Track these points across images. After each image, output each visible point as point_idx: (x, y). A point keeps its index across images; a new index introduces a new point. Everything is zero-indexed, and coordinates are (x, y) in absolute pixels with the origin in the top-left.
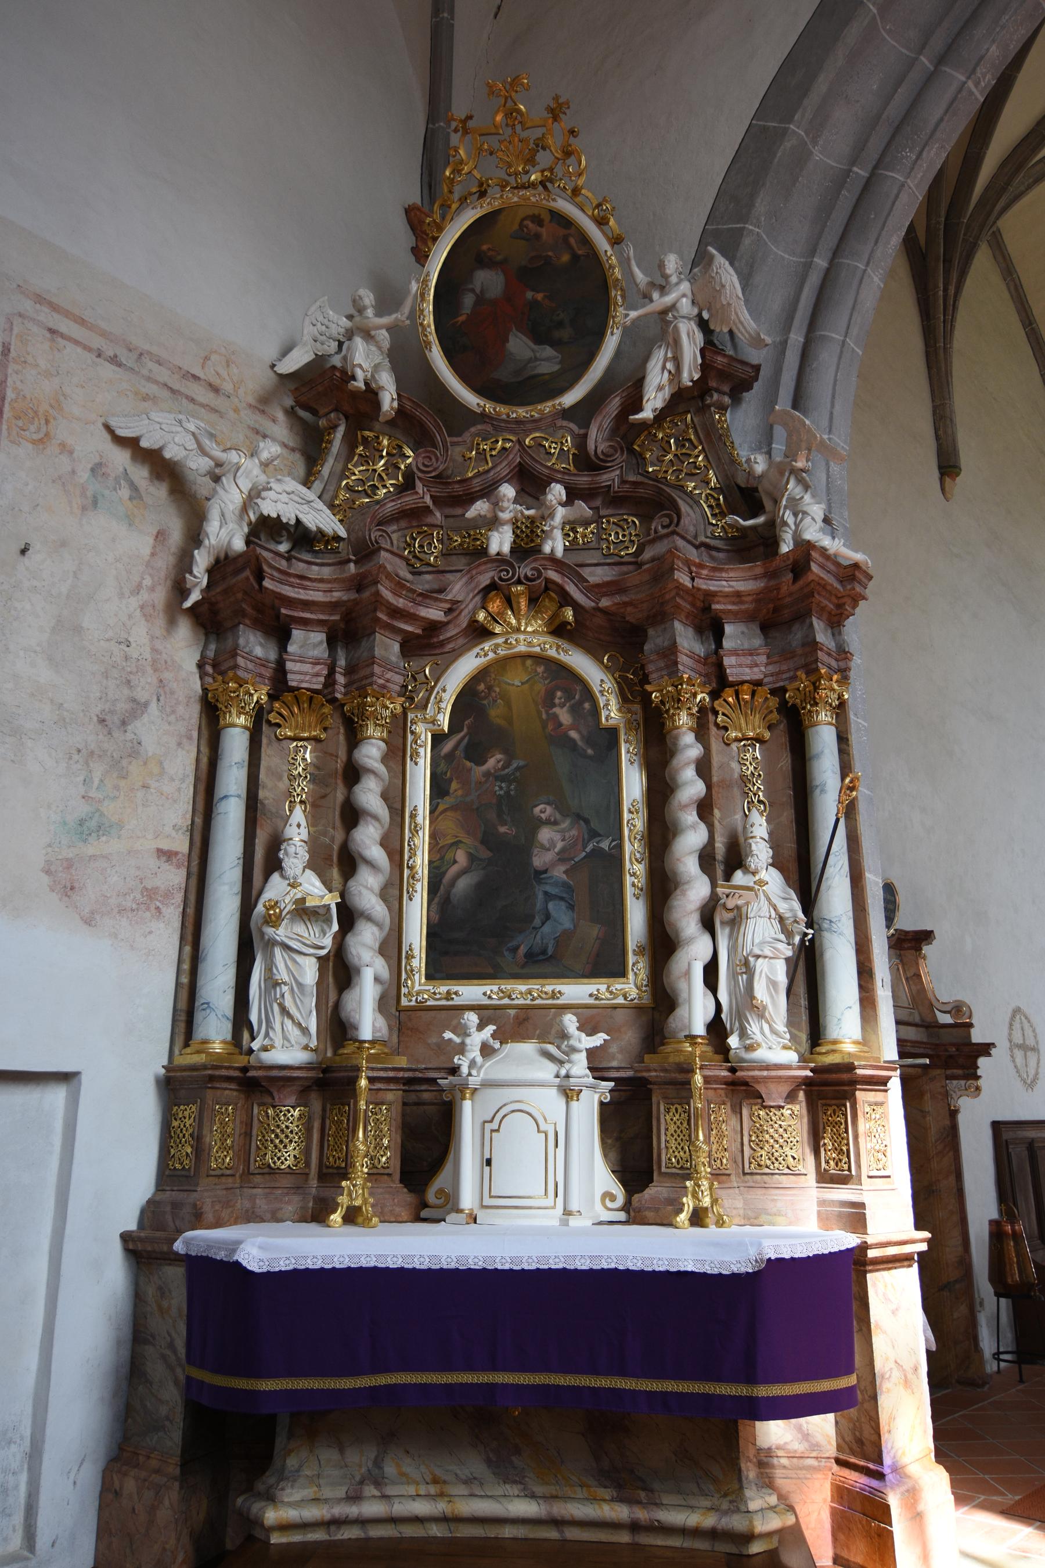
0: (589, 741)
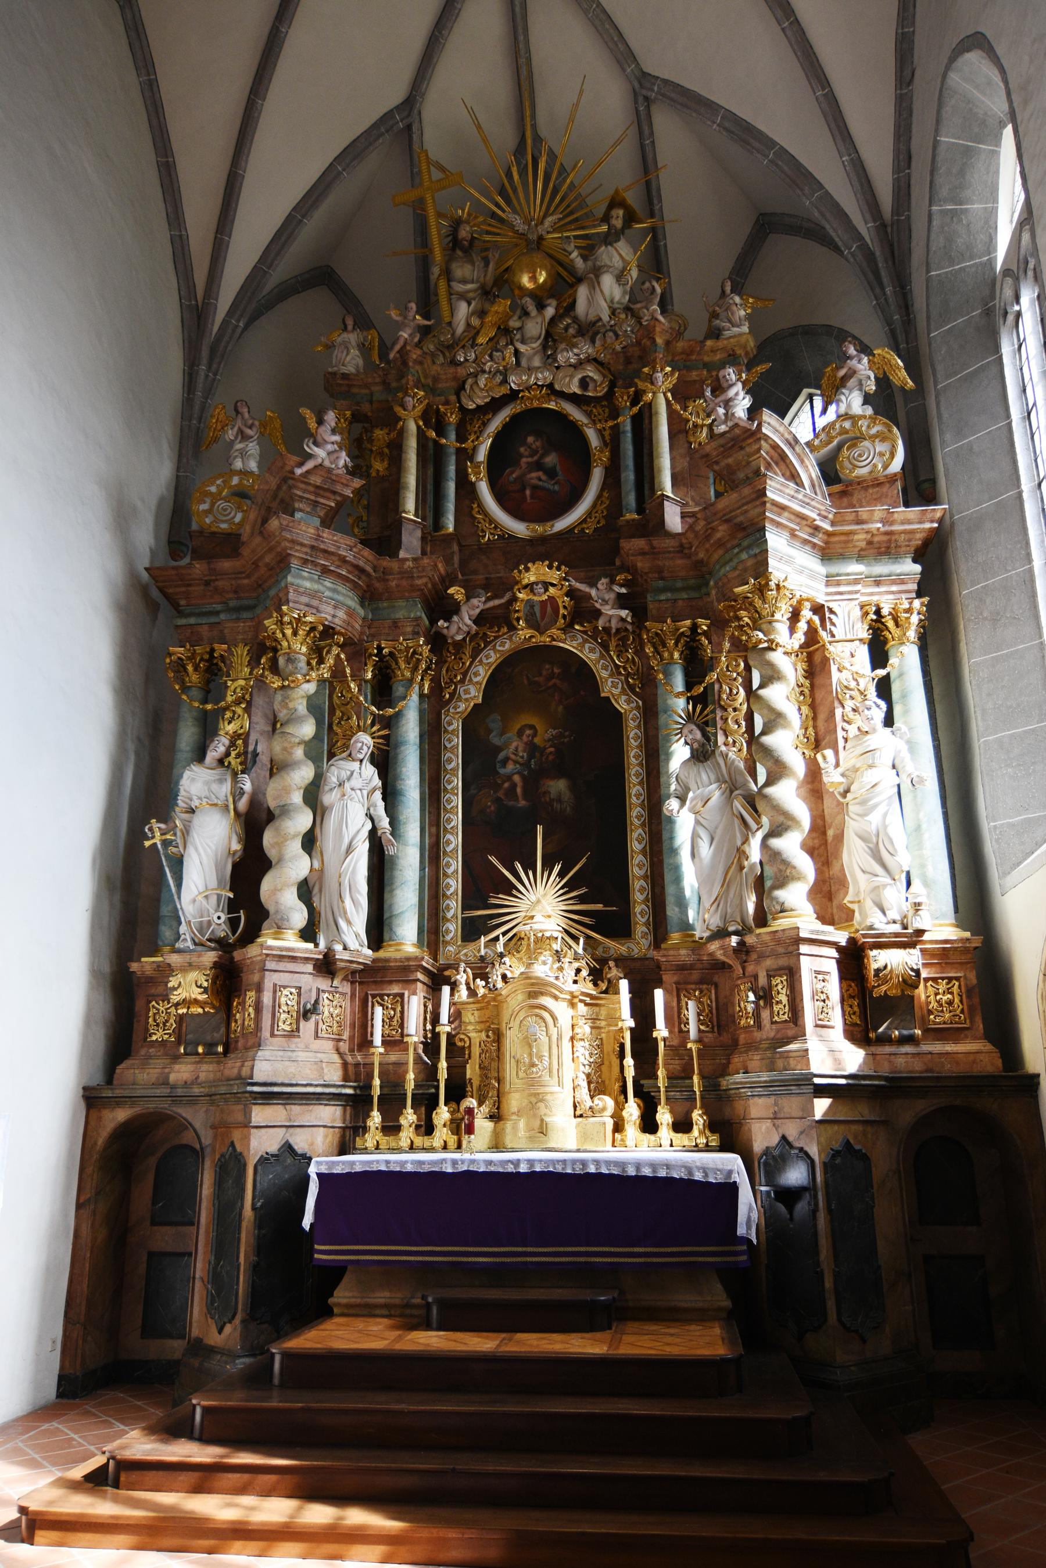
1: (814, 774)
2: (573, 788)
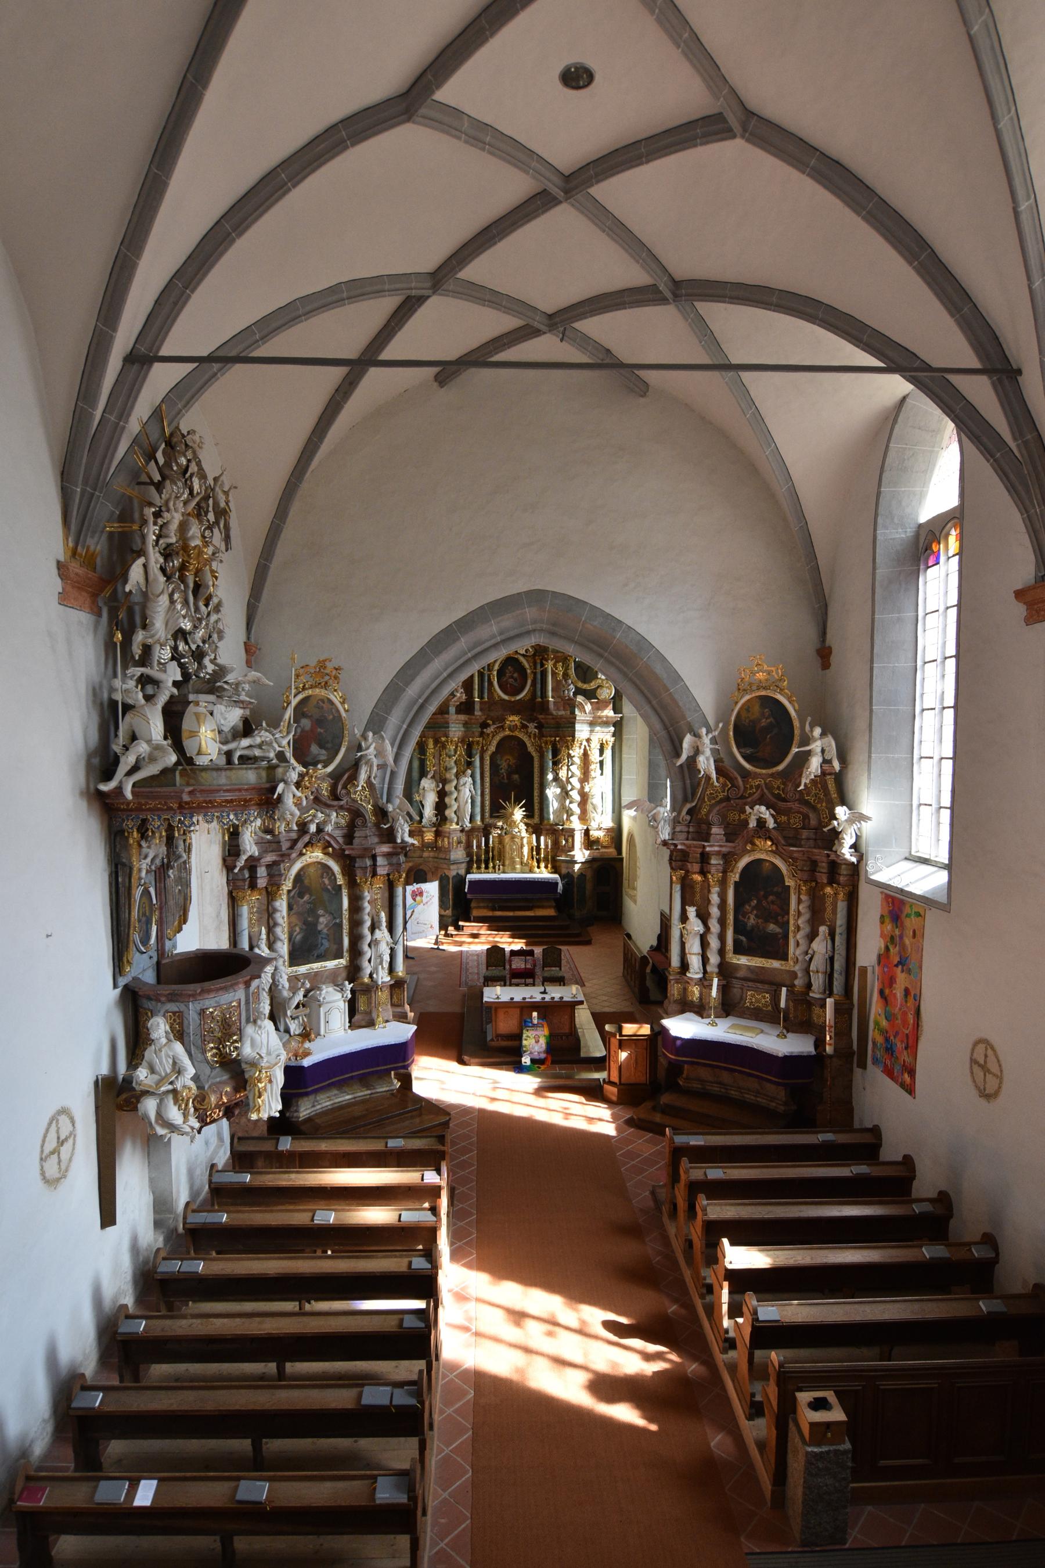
1: (582, 788)
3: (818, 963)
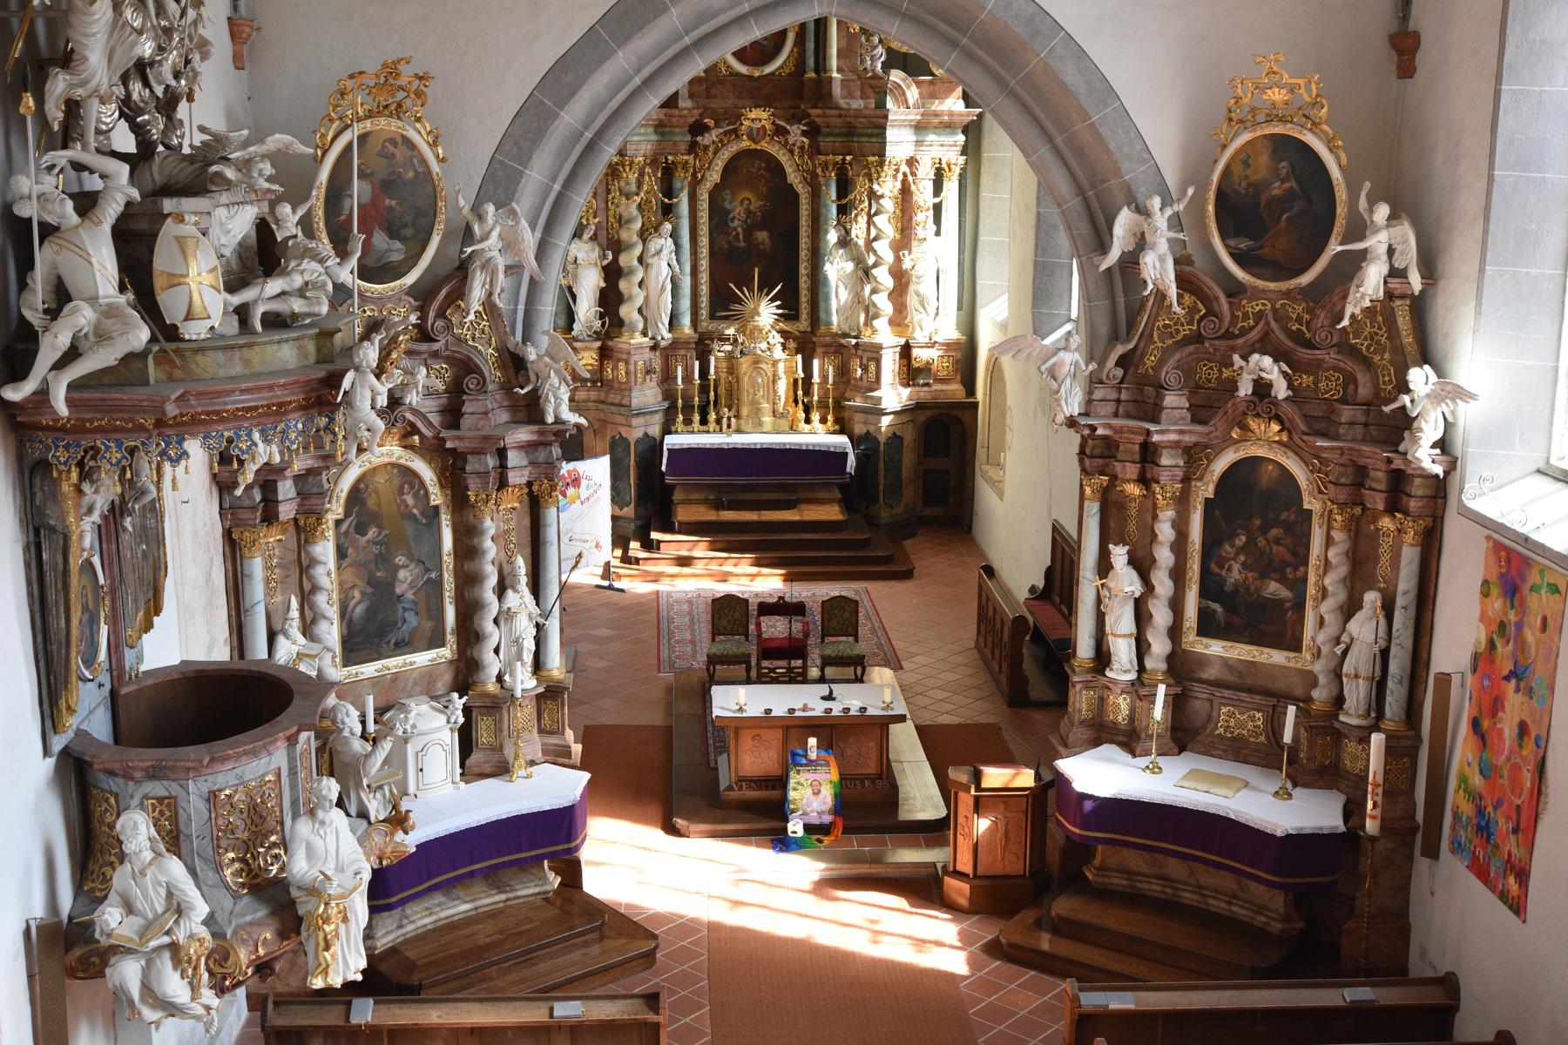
0: (423, 514)
1: (898, 260)
2: (771, 237)
3: (1359, 661)
